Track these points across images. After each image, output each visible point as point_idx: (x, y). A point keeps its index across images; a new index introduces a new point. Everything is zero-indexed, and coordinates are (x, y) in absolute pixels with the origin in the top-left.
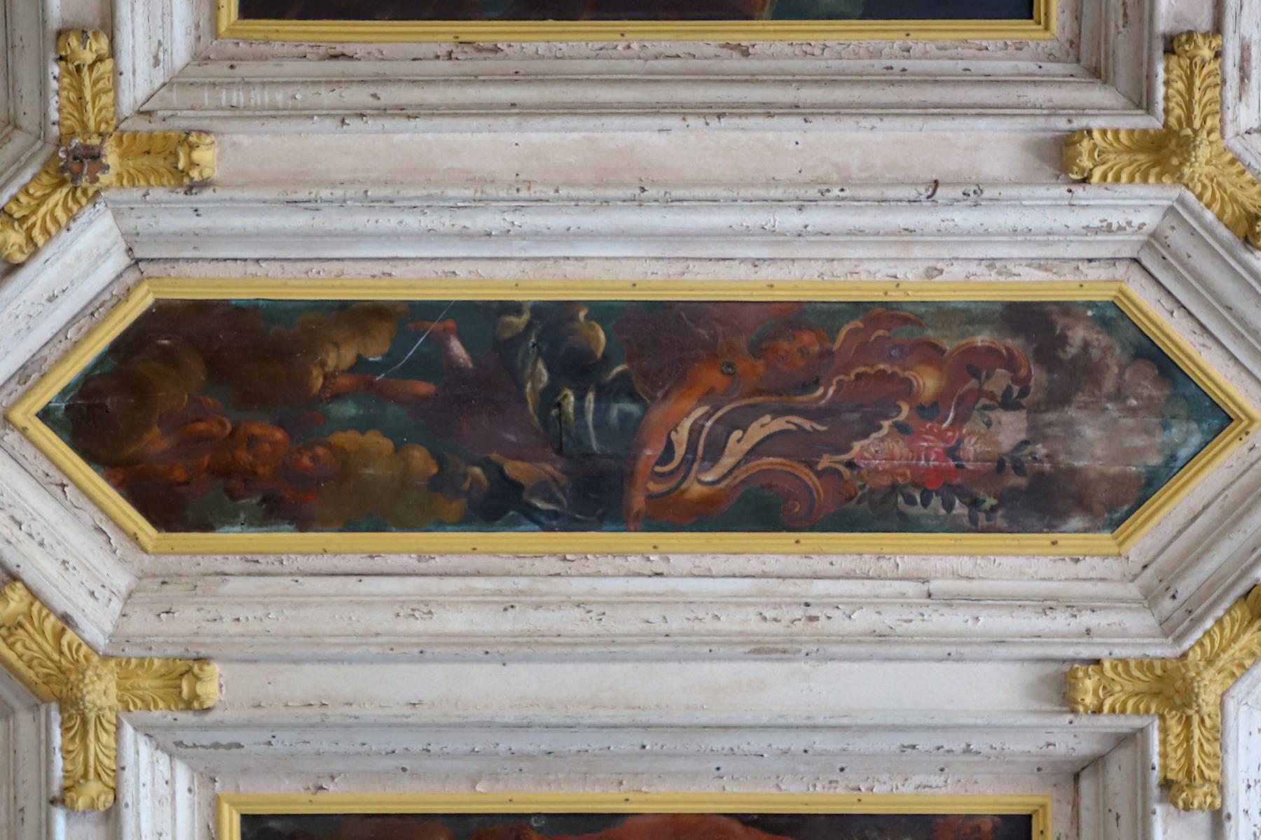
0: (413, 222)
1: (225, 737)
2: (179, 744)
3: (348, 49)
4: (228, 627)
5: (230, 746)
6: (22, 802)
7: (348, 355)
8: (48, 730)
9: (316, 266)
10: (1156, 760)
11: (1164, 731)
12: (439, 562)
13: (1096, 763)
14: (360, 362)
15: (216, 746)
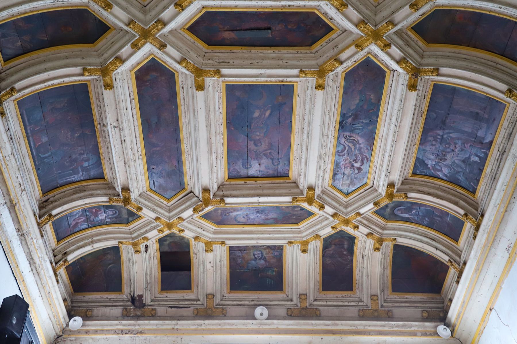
0: (395, 112)
1: (310, 88)
2: (309, 82)
3: (426, 98)
4: (330, 89)
5: (308, 88)
6: (301, 61)
7: (372, 98)
8: (314, 68)
9: (389, 94)
10: (299, 197)
11: (304, 198)
12: (336, 111)
13: (298, 187)
14: (371, 99)
15: (308, 87)
